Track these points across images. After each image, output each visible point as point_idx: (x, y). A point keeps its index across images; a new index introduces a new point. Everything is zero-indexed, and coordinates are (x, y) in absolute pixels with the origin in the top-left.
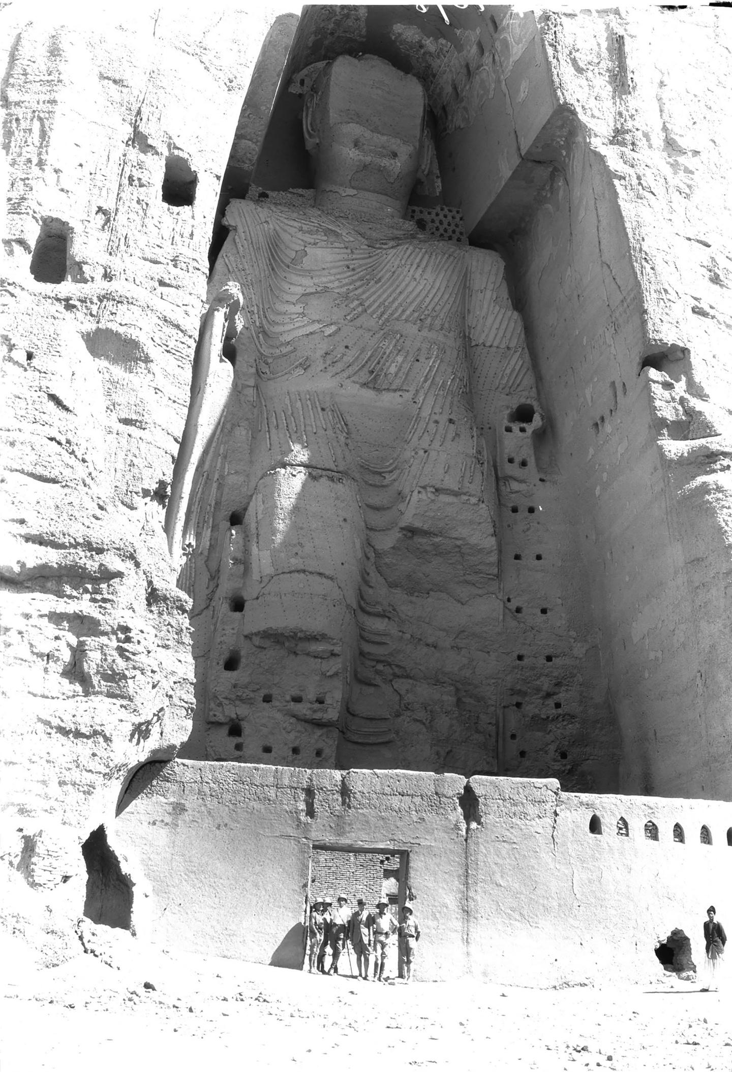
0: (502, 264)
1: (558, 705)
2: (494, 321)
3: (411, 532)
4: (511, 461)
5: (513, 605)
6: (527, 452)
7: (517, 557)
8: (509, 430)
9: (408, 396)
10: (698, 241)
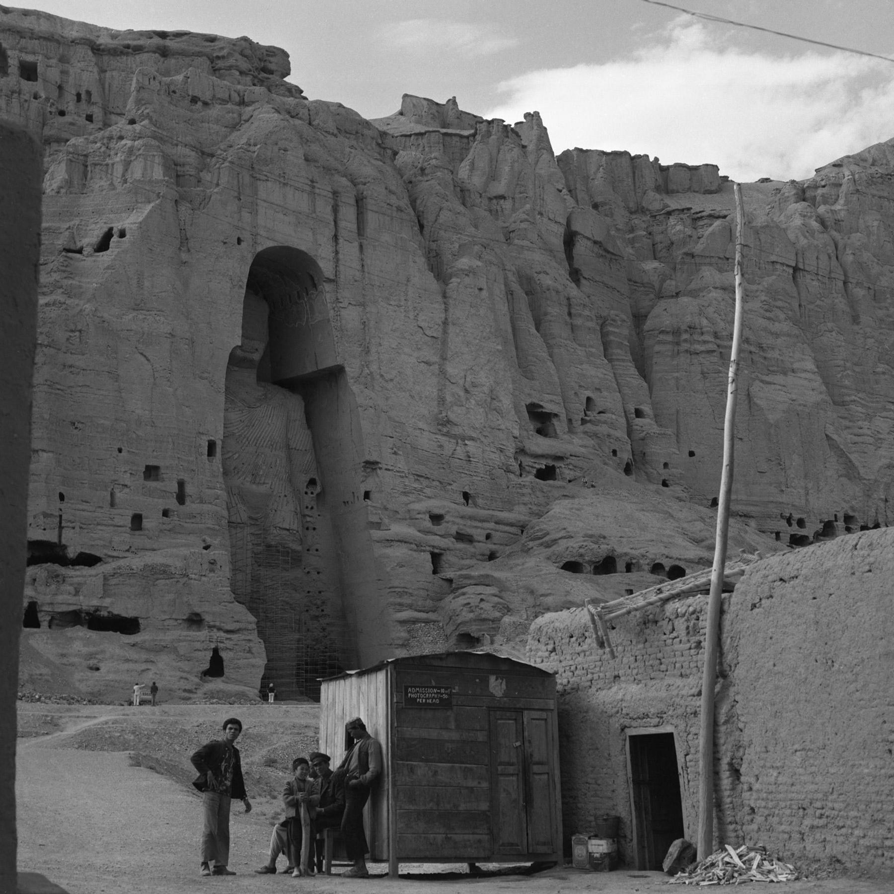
0: (303, 404)
1: (323, 611)
2: (301, 438)
3: (269, 546)
4: (307, 507)
5: (307, 570)
6: (313, 503)
7: (308, 550)
8: (306, 493)
9: (268, 486)
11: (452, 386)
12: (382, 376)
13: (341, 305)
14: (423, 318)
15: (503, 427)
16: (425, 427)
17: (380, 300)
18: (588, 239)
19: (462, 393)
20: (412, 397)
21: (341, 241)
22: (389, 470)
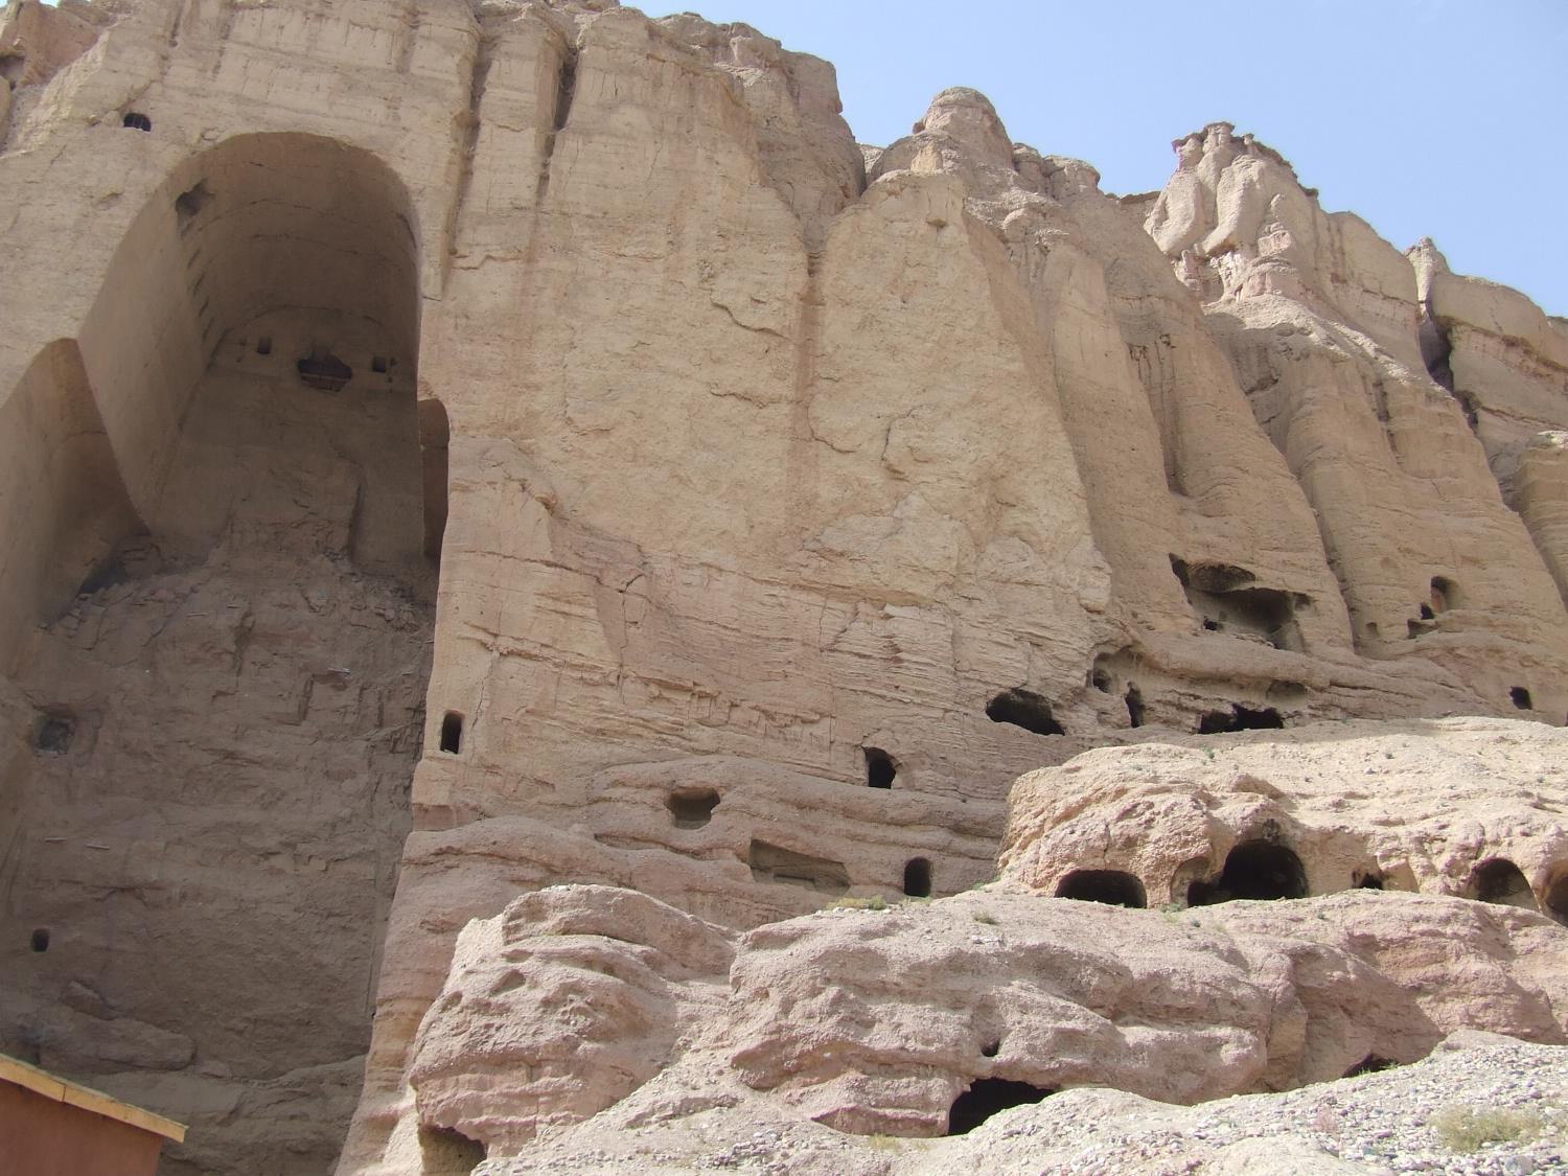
10: (542, 561)
11: (836, 458)
12: (569, 421)
13: (461, 263)
14: (733, 284)
15: (1038, 576)
16: (729, 562)
17: (586, 246)
18: (1487, 333)
19: (876, 478)
20: (684, 481)
21: (486, 130)
22: (530, 657)
